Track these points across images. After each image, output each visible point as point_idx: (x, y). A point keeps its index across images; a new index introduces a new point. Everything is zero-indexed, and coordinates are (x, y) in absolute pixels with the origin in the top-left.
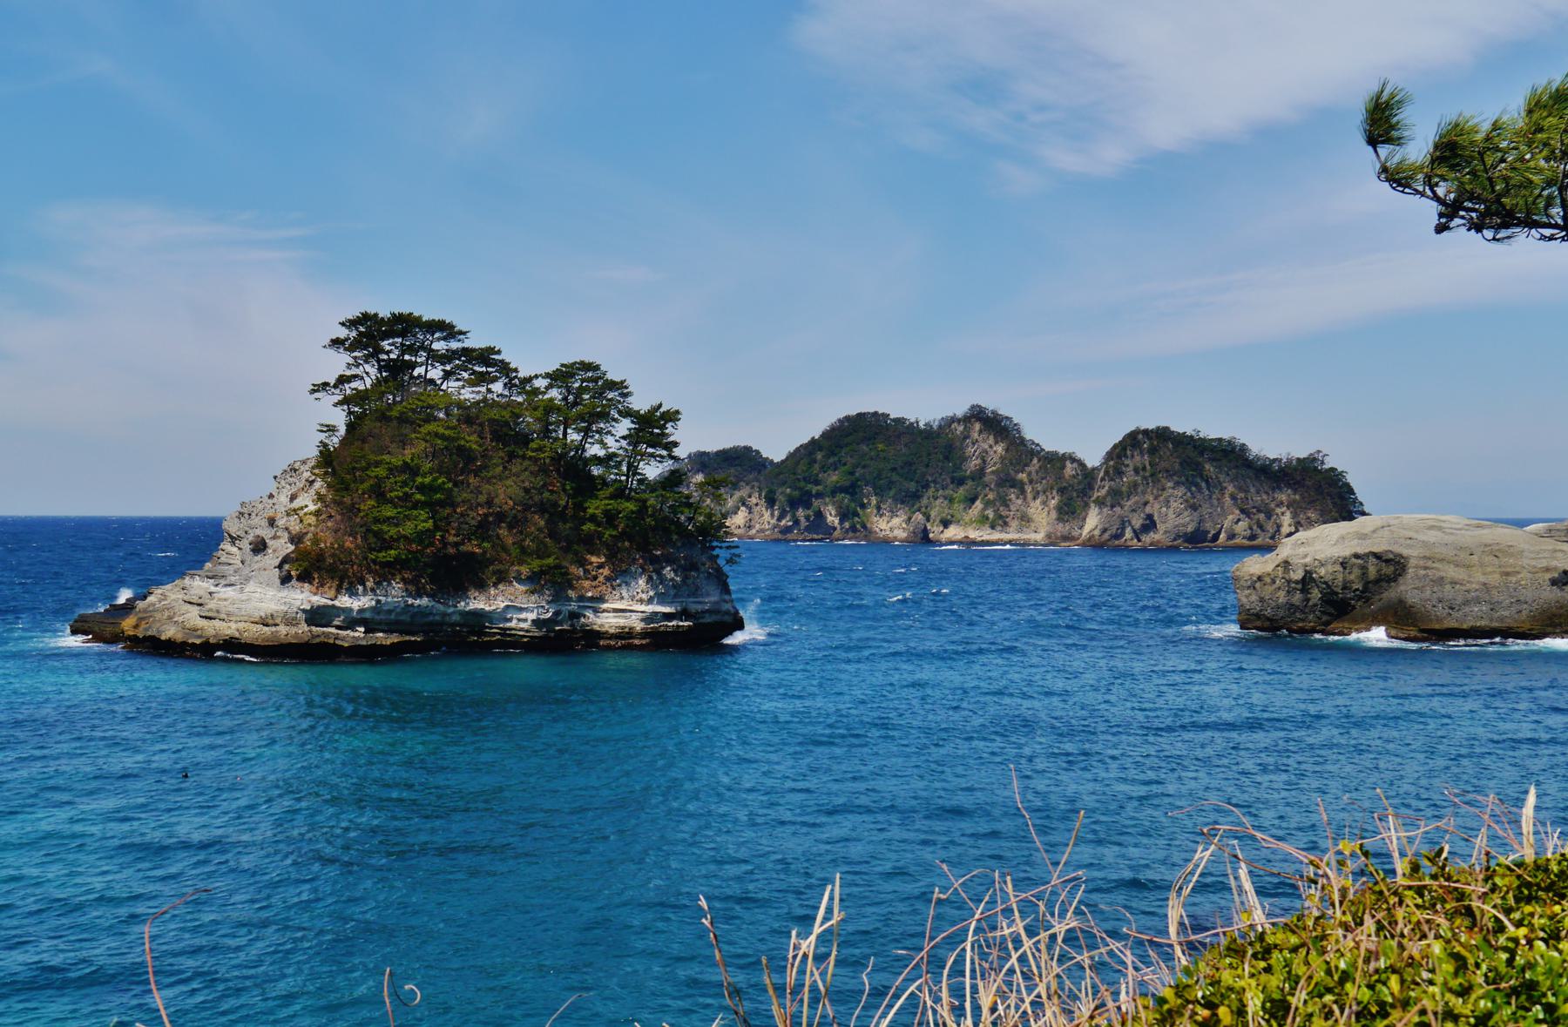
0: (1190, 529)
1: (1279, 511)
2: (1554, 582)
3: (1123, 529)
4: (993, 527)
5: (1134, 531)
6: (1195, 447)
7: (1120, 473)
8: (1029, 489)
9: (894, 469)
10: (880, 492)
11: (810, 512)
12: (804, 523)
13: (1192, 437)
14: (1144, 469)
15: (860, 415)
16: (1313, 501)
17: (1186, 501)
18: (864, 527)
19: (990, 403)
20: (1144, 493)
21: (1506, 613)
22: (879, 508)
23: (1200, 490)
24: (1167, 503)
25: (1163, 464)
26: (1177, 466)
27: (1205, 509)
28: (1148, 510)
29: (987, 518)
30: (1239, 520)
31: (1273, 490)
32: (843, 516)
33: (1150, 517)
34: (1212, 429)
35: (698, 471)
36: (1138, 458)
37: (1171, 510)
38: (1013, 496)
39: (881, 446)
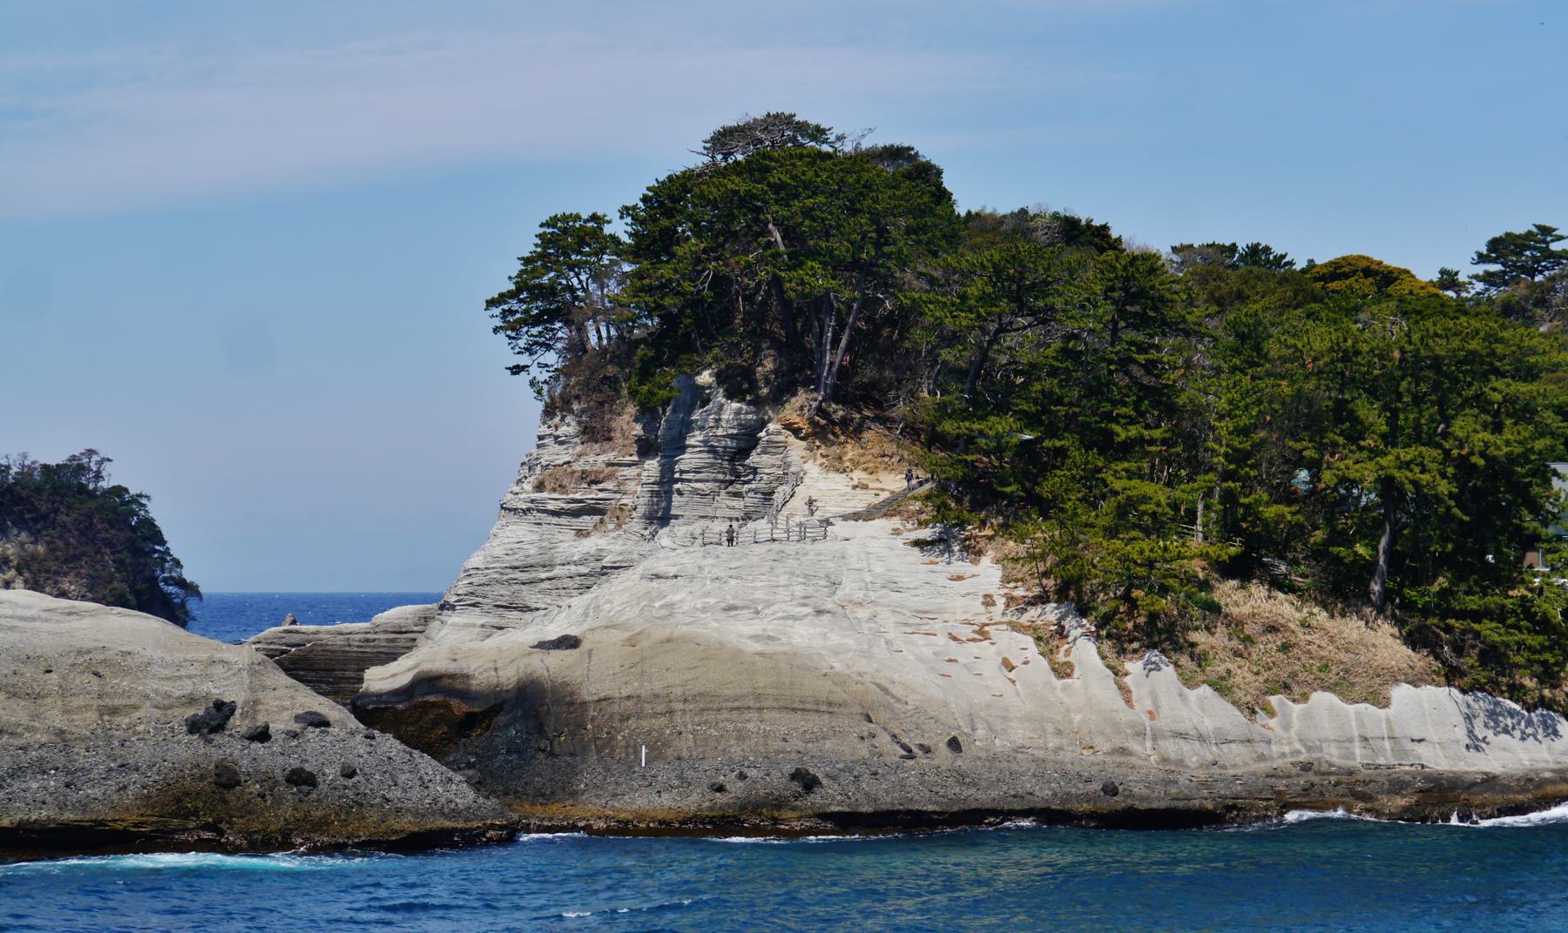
2: (194, 726)
16: (76, 558)
21: (96, 792)
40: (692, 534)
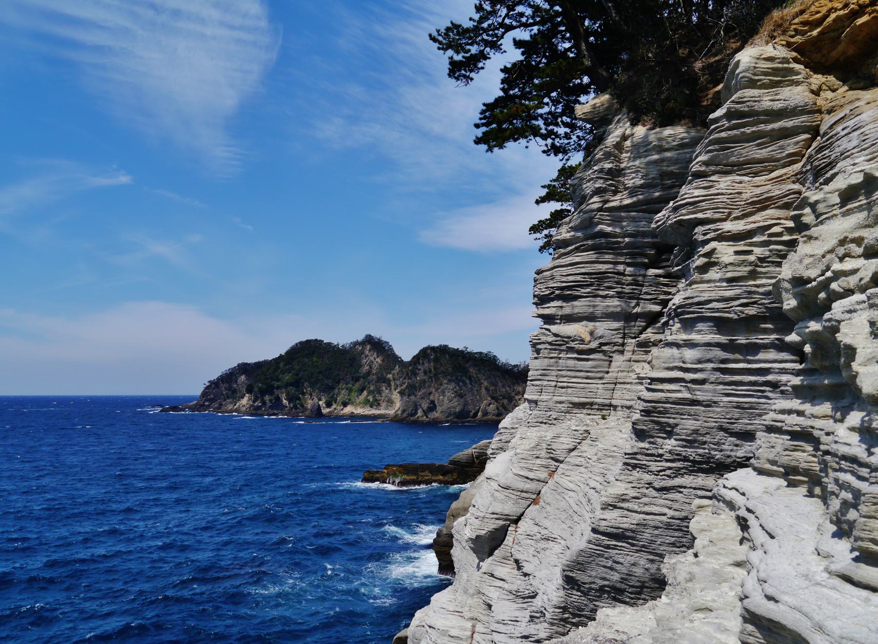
0: (457, 410)
1: (517, 397)
3: (416, 410)
4: (371, 407)
5: (424, 411)
6: (463, 358)
7: (416, 375)
8: (392, 383)
9: (320, 373)
10: (312, 385)
11: (272, 397)
12: (268, 404)
13: (462, 352)
14: (430, 371)
15: (308, 341)
17: (456, 392)
18: (302, 406)
19: (376, 334)
20: (429, 387)
22: (311, 395)
23: (465, 384)
24: (443, 392)
25: (442, 369)
26: (450, 369)
27: (469, 398)
28: (431, 397)
29: (369, 401)
30: (490, 404)
31: (514, 384)
32: (290, 400)
33: (433, 402)
34: (475, 347)
35: (242, 374)
36: (426, 365)
37: (446, 398)
38: (384, 388)
39: (315, 359)
40: (550, 450)
